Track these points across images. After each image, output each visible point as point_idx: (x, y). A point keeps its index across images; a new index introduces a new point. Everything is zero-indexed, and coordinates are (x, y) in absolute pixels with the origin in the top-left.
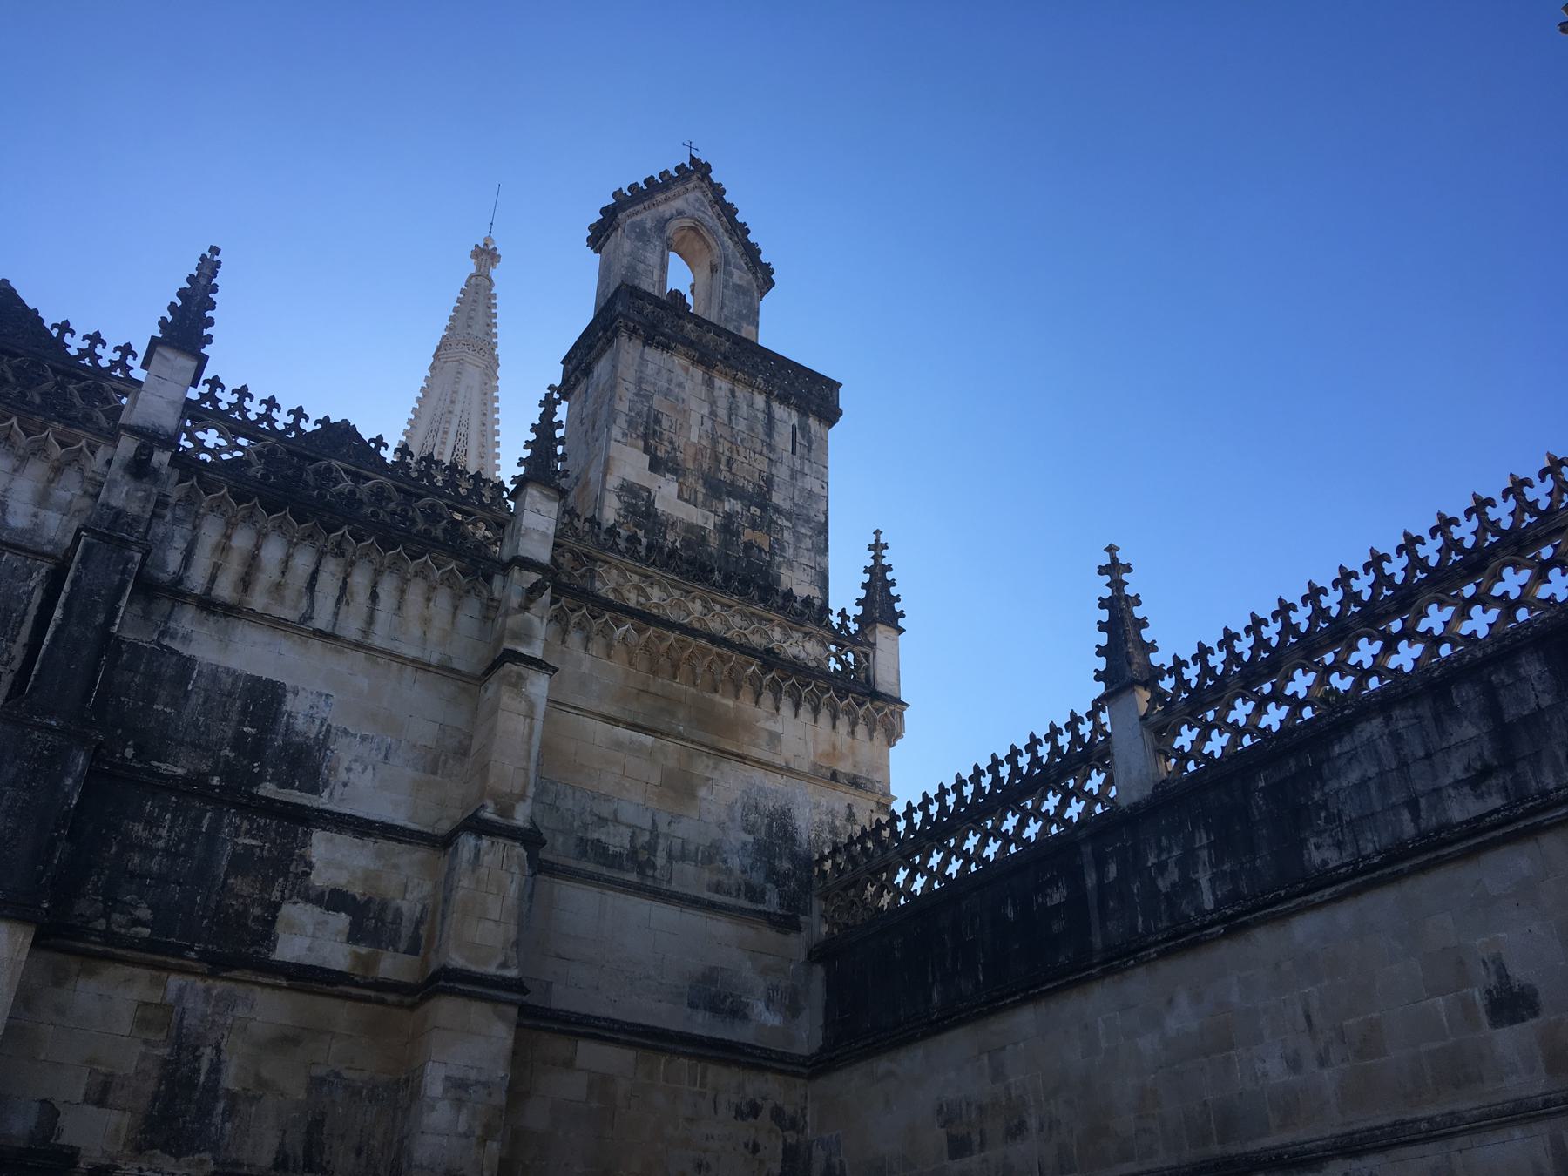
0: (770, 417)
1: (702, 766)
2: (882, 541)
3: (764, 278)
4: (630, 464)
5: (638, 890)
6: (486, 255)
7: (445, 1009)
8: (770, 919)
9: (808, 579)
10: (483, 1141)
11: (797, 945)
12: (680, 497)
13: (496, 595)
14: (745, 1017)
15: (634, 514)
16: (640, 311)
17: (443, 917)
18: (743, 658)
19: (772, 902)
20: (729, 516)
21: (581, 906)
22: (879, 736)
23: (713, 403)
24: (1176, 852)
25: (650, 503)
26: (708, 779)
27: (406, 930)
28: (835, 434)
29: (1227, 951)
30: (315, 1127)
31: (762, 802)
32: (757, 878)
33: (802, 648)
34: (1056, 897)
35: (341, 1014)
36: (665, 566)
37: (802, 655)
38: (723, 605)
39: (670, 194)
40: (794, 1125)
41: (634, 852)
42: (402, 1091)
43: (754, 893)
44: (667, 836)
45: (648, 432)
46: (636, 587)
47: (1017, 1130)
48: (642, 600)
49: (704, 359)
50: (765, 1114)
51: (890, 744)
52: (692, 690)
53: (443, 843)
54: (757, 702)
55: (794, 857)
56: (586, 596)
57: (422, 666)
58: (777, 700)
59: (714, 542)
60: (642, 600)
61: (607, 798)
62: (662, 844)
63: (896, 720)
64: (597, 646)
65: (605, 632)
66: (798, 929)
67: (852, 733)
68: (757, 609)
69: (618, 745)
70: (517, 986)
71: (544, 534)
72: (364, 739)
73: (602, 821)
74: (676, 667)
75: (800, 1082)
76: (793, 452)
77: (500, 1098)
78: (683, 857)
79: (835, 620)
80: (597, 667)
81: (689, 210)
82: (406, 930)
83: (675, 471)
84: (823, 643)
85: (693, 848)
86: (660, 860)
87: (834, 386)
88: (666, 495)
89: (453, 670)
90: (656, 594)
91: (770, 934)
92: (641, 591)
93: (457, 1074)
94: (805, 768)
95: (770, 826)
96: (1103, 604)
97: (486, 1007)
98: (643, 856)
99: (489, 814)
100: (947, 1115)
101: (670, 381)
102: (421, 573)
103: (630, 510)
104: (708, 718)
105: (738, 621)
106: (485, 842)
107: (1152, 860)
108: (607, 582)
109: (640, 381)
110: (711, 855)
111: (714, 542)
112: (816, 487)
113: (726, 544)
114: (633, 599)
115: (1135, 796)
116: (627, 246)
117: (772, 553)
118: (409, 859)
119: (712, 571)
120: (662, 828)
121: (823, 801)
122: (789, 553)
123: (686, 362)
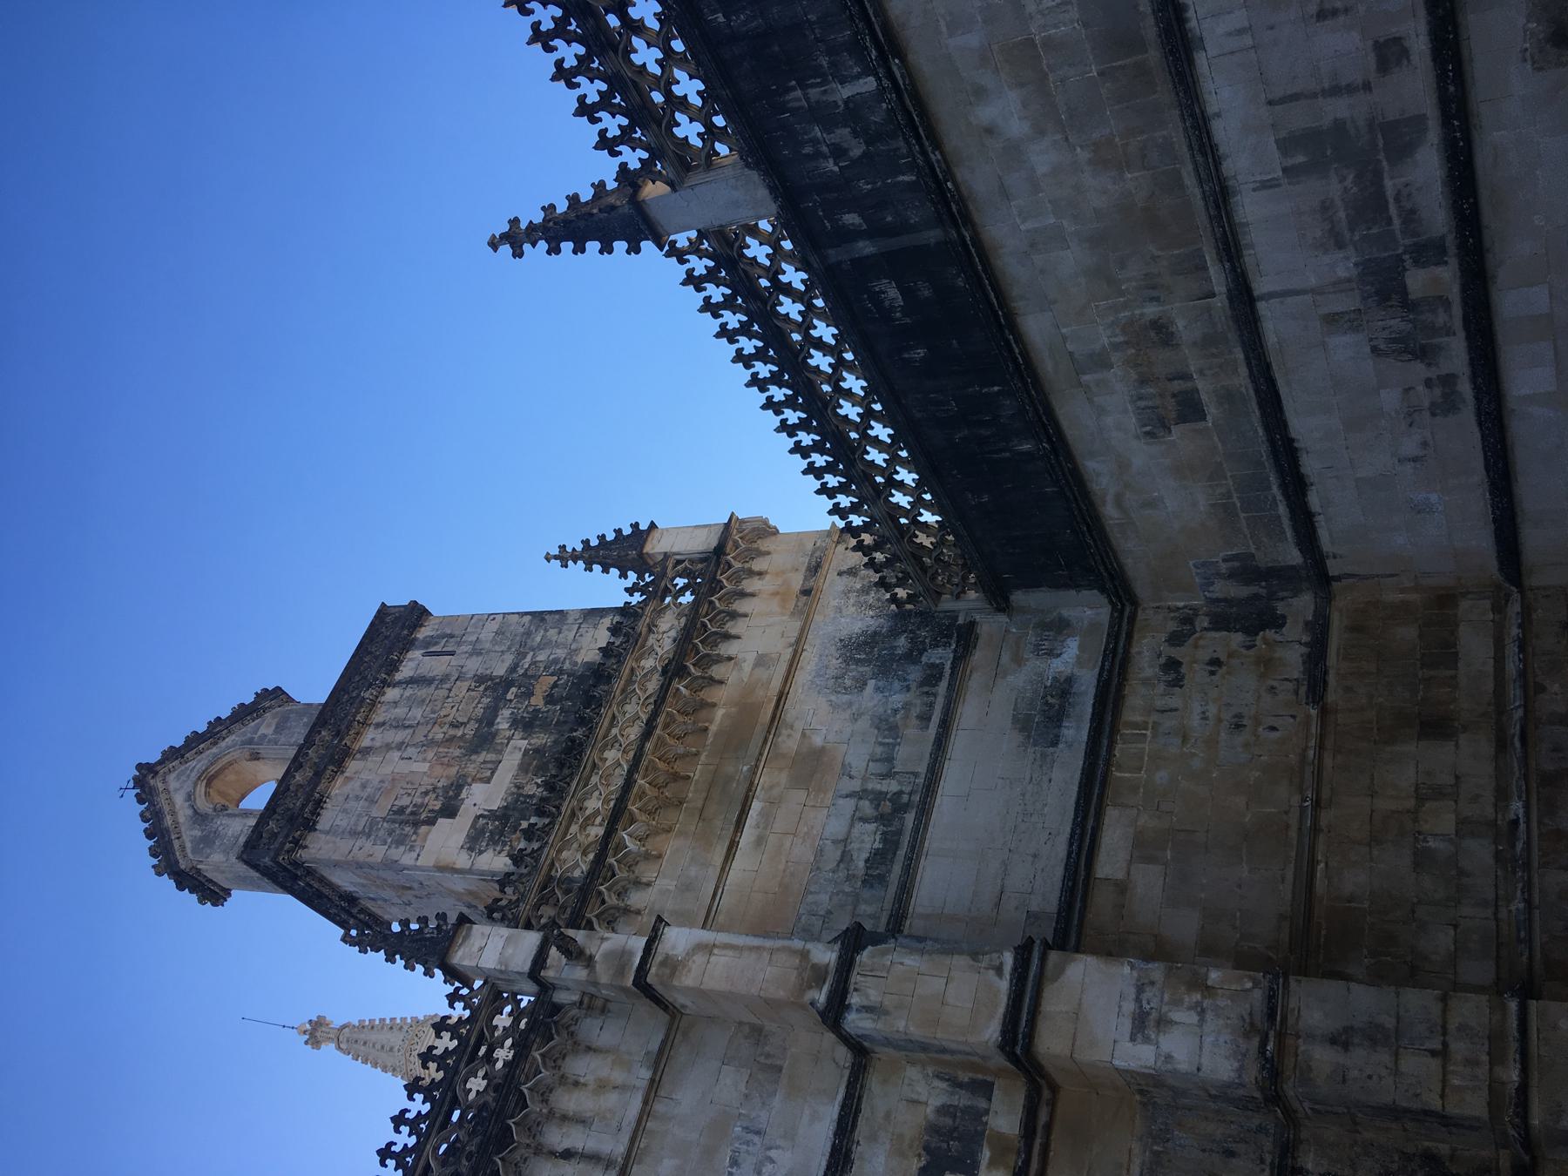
1: (789, 742)
2: (556, 552)
4: (445, 841)
5: (925, 810)
6: (316, 1033)
7: (1051, 1043)
8: (962, 656)
9: (591, 631)
10: (1208, 990)
11: (990, 625)
12: (488, 780)
13: (576, 998)
14: (1070, 680)
15: (502, 834)
16: (274, 835)
17: (944, 1050)
18: (669, 699)
19: (942, 655)
21: (942, 881)
22: (764, 545)
23: (388, 747)
24: (817, 132)
25: (492, 816)
26: (804, 735)
27: (963, 1099)
28: (438, 608)
29: (921, 55)
31: (831, 672)
32: (915, 674)
33: (666, 631)
34: (893, 293)
37: (673, 633)
38: (612, 725)
39: (166, 808)
40: (1188, 620)
41: (881, 818)
43: (932, 676)
44: (864, 779)
45: (412, 820)
46: (583, 827)
47: (1162, 332)
48: (599, 820)
49: (338, 759)
50: (1175, 653)
51: (775, 532)
52: (703, 758)
53: (861, 1052)
54: (721, 682)
55: (894, 633)
56: (587, 889)
57: (653, 1088)
58: (719, 660)
59: (541, 739)
60: (599, 820)
61: (820, 853)
62: (875, 785)
63: (748, 527)
64: (647, 872)
65: (630, 863)
66: (972, 624)
67: (760, 574)
68: (617, 686)
69: (760, 841)
70: (1023, 953)
71: (508, 940)
72: (735, 1162)
73: (846, 857)
74: (676, 777)
75: (1141, 615)
76: (452, 654)
77: (1157, 971)
78: (889, 759)
79: (637, 598)
80: (671, 871)
81: (188, 787)
82: (963, 1099)
83: (459, 788)
84: (660, 612)
85: (879, 750)
86: (892, 786)
87: (383, 611)
88: (484, 797)
89: (661, 1051)
90: (593, 804)
91: (978, 656)
92: (588, 821)
93: (1127, 1025)
94: (798, 624)
95: (858, 662)
96: (554, 250)
97: (1049, 993)
98: (887, 807)
99: (821, 997)
100: (1155, 426)
101: (357, 798)
102: (544, 1094)
103: (497, 839)
104: (734, 739)
105: (631, 709)
106: (854, 999)
107: (831, 165)
108: (574, 862)
109: (354, 834)
110: (888, 727)
111: (541, 739)
112: (493, 626)
113: (545, 726)
114: (597, 831)
115: (763, 193)
116: (217, 857)
117: (561, 672)
118: (880, 1097)
119: (573, 740)
120: (856, 785)
121: (835, 603)
122: (561, 653)
123: (340, 780)
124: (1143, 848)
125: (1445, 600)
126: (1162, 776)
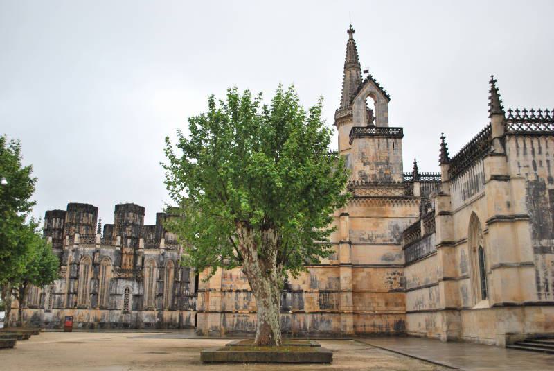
0: (388, 143)
1: (380, 221)
3: (387, 98)
7: (341, 269)
8: (395, 244)
11: (400, 248)
12: (370, 169)
19: (395, 241)
20: (380, 170)
23: (375, 145)
25: (364, 173)
28: (402, 140)
30: (330, 284)
32: (392, 237)
35: (330, 269)
36: (368, 186)
41: (369, 239)
42: (338, 278)
59: (378, 177)
61: (363, 231)
73: (363, 234)
86: (374, 238)
88: (368, 170)
90: (368, 192)
91: (395, 247)
124: (368, 273)
125: (405, 305)
126: (378, 274)
